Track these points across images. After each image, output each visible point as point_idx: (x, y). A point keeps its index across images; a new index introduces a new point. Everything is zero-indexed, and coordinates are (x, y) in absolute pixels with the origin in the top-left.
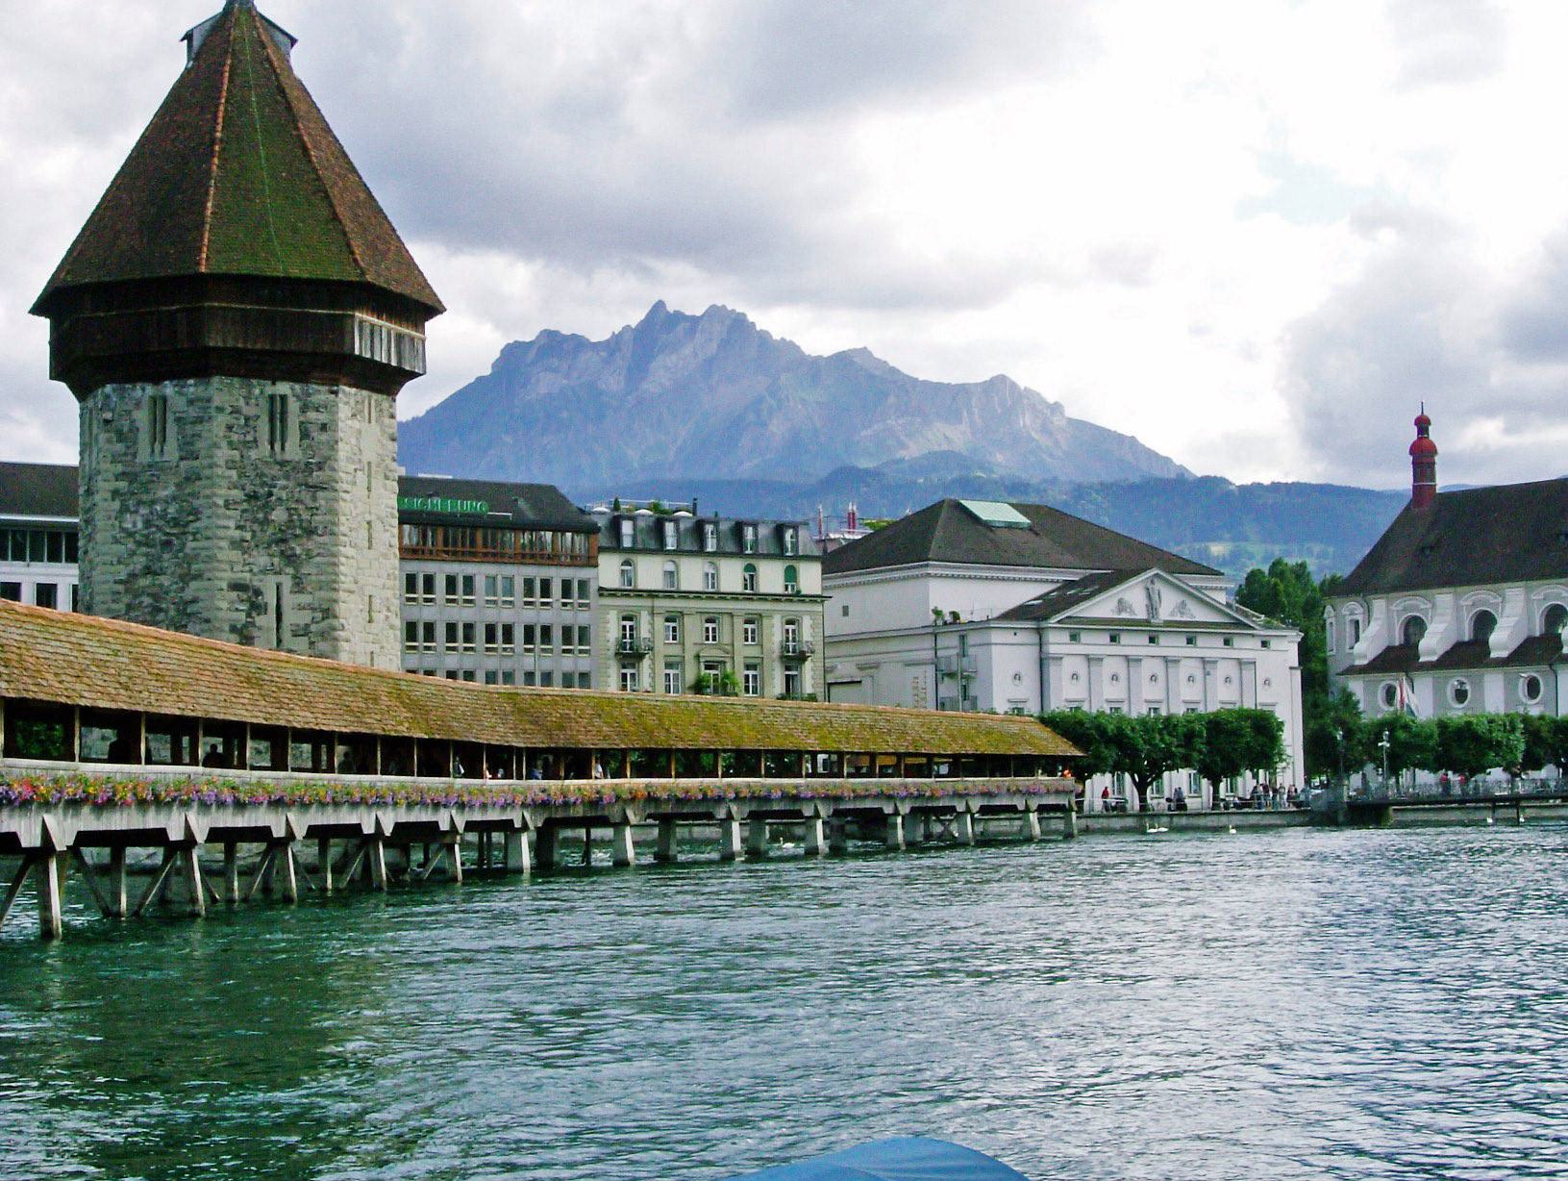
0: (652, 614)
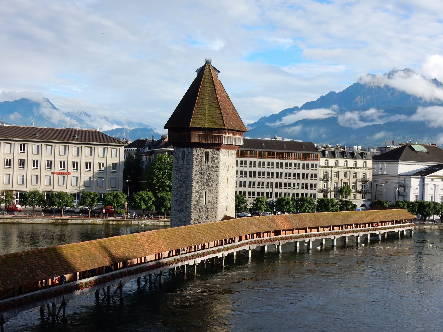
0: (331, 171)
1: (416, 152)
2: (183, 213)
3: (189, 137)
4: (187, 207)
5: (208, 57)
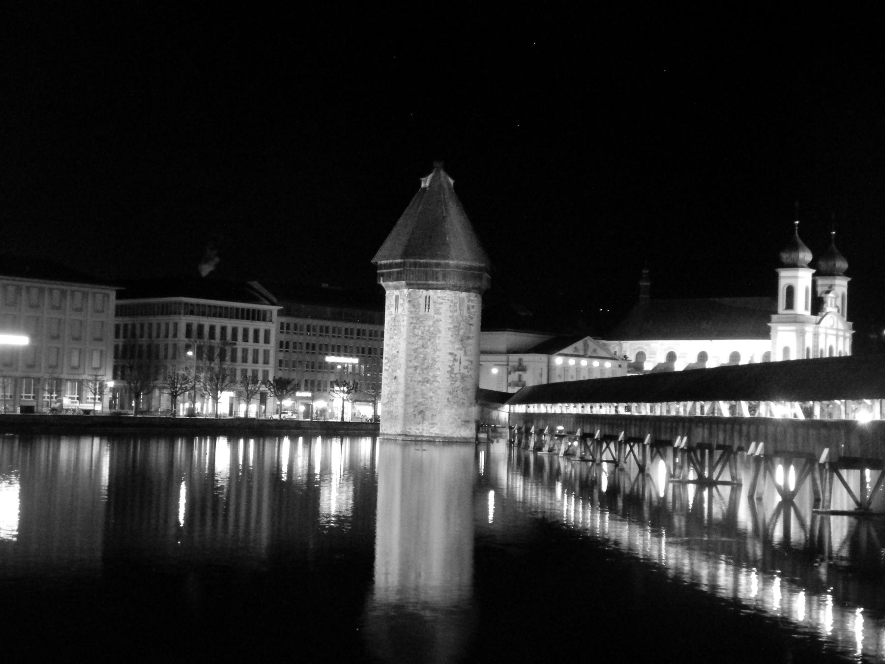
2: (428, 385)
4: (435, 376)
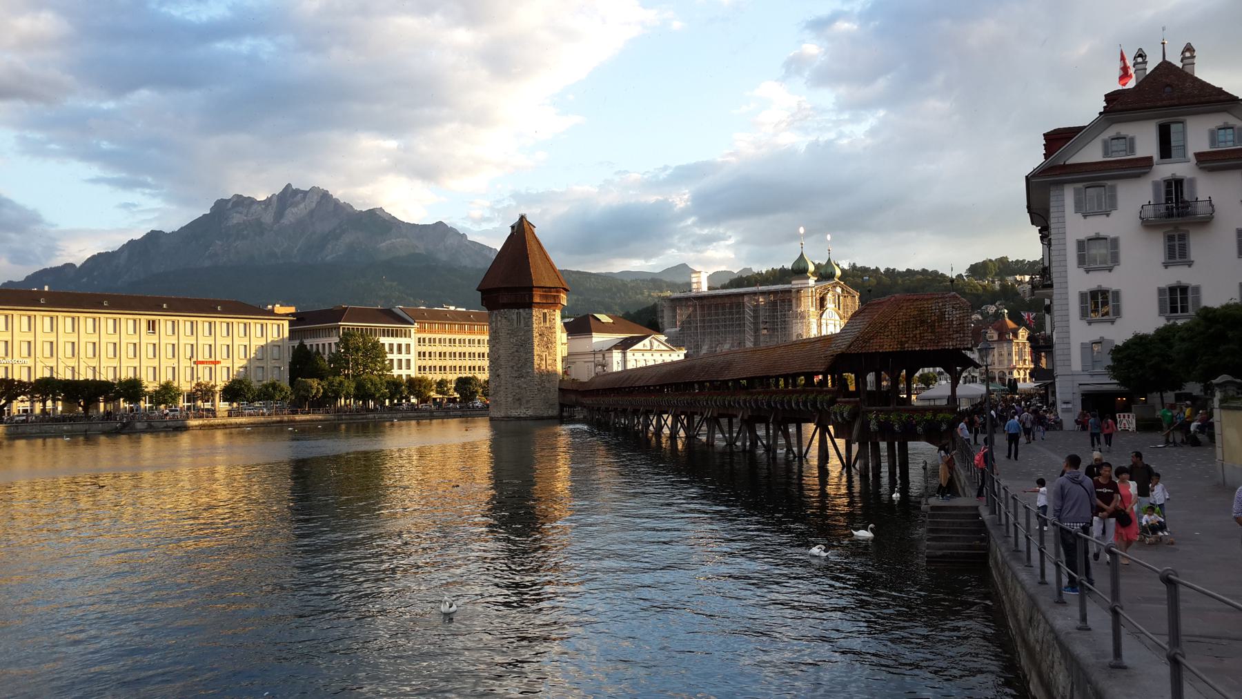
1: (603, 323)
2: (522, 379)
3: (531, 297)
4: (528, 372)
5: (523, 212)
